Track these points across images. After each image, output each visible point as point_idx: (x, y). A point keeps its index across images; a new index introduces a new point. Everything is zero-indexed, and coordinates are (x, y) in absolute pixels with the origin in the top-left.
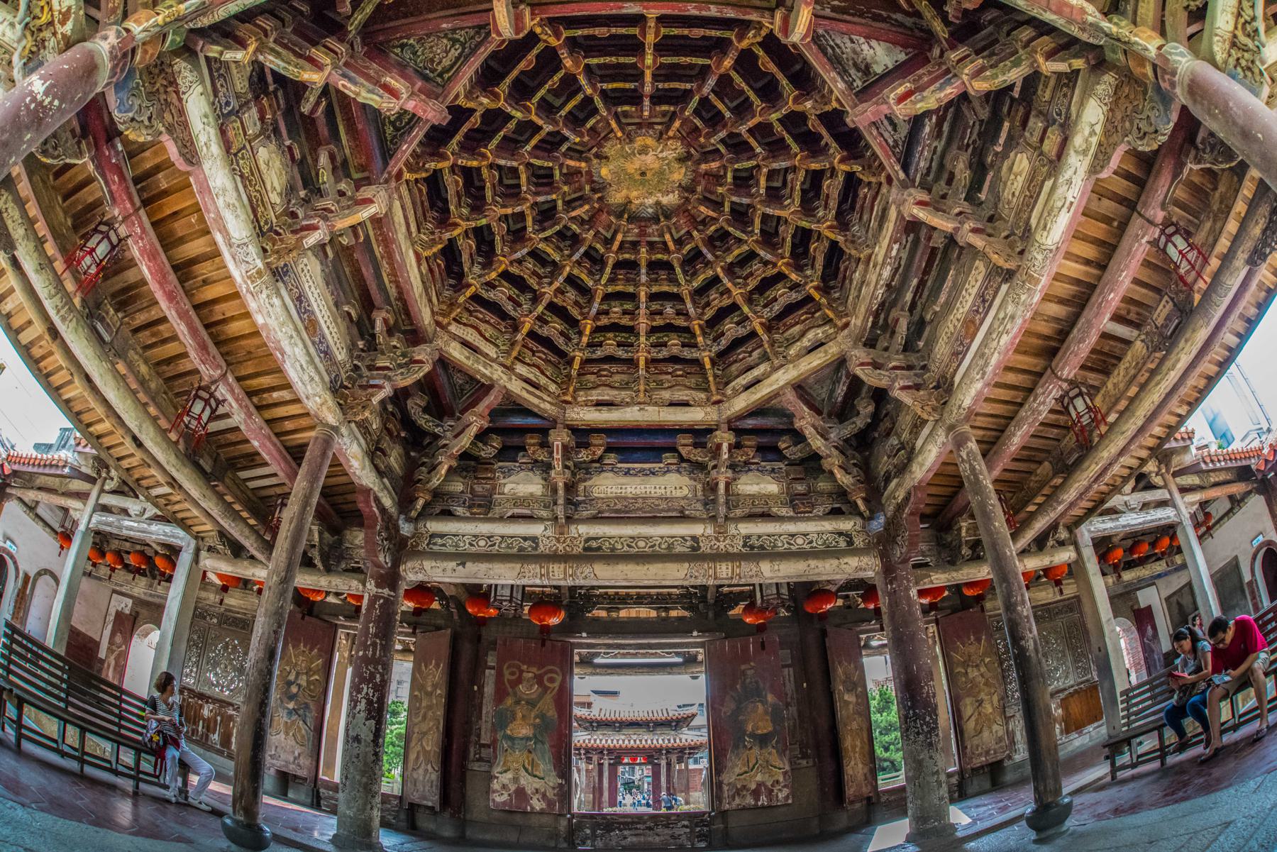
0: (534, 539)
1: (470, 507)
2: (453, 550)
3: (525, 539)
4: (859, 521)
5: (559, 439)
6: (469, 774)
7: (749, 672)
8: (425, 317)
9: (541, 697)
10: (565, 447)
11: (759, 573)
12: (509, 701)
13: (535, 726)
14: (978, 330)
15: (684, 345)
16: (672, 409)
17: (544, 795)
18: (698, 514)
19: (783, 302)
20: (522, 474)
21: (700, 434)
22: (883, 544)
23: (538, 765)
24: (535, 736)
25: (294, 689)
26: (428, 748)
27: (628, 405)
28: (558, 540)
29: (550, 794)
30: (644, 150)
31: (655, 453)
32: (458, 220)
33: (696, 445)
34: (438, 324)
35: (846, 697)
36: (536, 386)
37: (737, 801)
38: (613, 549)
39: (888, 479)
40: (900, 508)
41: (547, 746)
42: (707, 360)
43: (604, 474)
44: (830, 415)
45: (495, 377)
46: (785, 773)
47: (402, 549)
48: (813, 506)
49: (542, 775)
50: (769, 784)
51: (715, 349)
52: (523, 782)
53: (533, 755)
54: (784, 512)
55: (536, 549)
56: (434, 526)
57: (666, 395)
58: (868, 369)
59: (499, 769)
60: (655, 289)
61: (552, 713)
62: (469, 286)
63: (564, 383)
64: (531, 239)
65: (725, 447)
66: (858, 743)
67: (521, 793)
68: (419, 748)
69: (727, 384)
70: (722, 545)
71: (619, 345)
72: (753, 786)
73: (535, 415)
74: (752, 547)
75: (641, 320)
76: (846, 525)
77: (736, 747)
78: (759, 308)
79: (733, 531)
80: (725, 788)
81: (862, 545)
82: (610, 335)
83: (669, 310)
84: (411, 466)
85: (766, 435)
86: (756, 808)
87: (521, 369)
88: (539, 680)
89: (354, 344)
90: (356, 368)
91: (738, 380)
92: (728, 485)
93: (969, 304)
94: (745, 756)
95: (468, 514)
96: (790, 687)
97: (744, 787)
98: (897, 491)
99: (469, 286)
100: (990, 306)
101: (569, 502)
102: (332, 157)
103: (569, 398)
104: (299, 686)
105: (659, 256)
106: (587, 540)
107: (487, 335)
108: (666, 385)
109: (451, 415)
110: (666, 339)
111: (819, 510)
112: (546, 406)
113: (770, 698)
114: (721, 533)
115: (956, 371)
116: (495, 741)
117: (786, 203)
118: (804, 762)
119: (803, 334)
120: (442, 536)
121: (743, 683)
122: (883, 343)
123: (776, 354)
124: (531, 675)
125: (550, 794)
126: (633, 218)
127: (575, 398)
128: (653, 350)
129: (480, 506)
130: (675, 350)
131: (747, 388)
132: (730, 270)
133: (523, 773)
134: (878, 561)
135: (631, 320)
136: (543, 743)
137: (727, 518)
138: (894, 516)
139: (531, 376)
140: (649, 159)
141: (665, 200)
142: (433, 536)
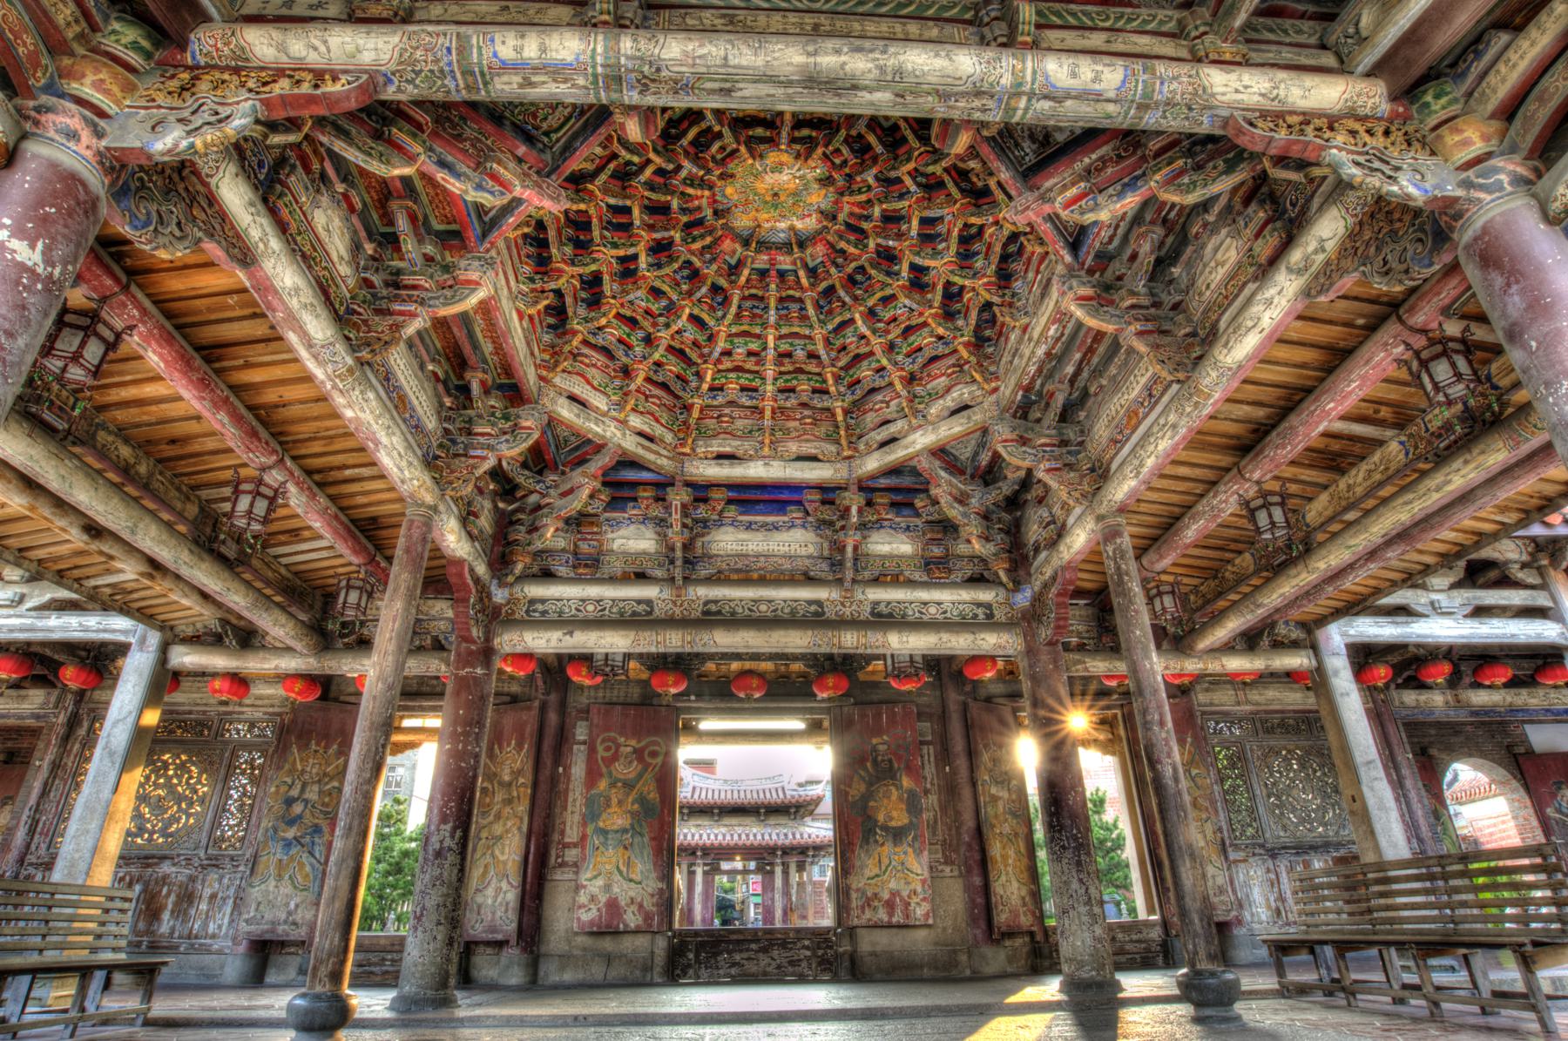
0: (649, 602)
1: (574, 567)
2: (555, 617)
3: (639, 602)
4: (1002, 593)
5: (678, 497)
8: (529, 376)
10: (684, 506)
12: (603, 784)
13: (633, 814)
14: (1140, 423)
15: (814, 391)
16: (799, 464)
17: (641, 906)
18: (823, 575)
19: (928, 353)
20: (632, 527)
21: (828, 493)
22: (1029, 619)
24: (632, 826)
25: (298, 808)
26: (502, 858)
27: (751, 459)
28: (674, 603)
29: (649, 904)
30: (778, 168)
31: (780, 506)
32: (562, 266)
33: (824, 502)
34: (541, 378)
35: (994, 791)
36: (650, 439)
37: (868, 914)
38: (733, 613)
39: (1037, 550)
40: (1046, 586)
41: (646, 839)
42: (839, 412)
43: (723, 529)
44: (973, 477)
45: (608, 434)
46: (923, 882)
47: (496, 618)
48: (950, 571)
49: (638, 878)
51: (849, 398)
54: (917, 576)
55: (650, 613)
56: (536, 590)
57: (794, 447)
58: (1012, 447)
59: (588, 875)
60: (784, 331)
61: (653, 796)
62: (575, 333)
63: (683, 430)
64: (644, 277)
65: (854, 510)
66: (1011, 853)
69: (860, 437)
70: (848, 611)
71: (743, 389)
72: (886, 896)
73: (649, 470)
74: (880, 615)
75: (768, 366)
76: (986, 595)
78: (900, 358)
79: (861, 597)
80: (854, 895)
81: (1003, 619)
82: (731, 375)
83: (800, 354)
84: (504, 523)
85: (900, 492)
87: (636, 421)
89: (441, 404)
90: (447, 431)
91: (872, 434)
92: (856, 548)
93: (1136, 392)
95: (572, 575)
98: (1047, 566)
99: (575, 333)
100: (1156, 403)
101: (686, 561)
102: (413, 218)
103: (687, 450)
104: (306, 801)
105: (791, 292)
106: (706, 603)
107: (595, 383)
108: (794, 434)
109: (554, 468)
110: (795, 382)
111: (957, 576)
112: (662, 461)
114: (847, 599)
115: (1112, 458)
116: (584, 837)
117: (940, 247)
118: (948, 869)
119: (948, 390)
120: (543, 601)
122: (1035, 414)
123: (916, 412)
126: (764, 245)
127: (693, 450)
128: (780, 396)
129: (586, 566)
130: (805, 398)
131: (883, 444)
132: (871, 314)
133: (617, 877)
134: (1021, 640)
135: (757, 364)
136: (642, 835)
137: (854, 581)
138: (1041, 593)
139: (646, 429)
140: (784, 177)
141: (799, 225)
142: (532, 602)
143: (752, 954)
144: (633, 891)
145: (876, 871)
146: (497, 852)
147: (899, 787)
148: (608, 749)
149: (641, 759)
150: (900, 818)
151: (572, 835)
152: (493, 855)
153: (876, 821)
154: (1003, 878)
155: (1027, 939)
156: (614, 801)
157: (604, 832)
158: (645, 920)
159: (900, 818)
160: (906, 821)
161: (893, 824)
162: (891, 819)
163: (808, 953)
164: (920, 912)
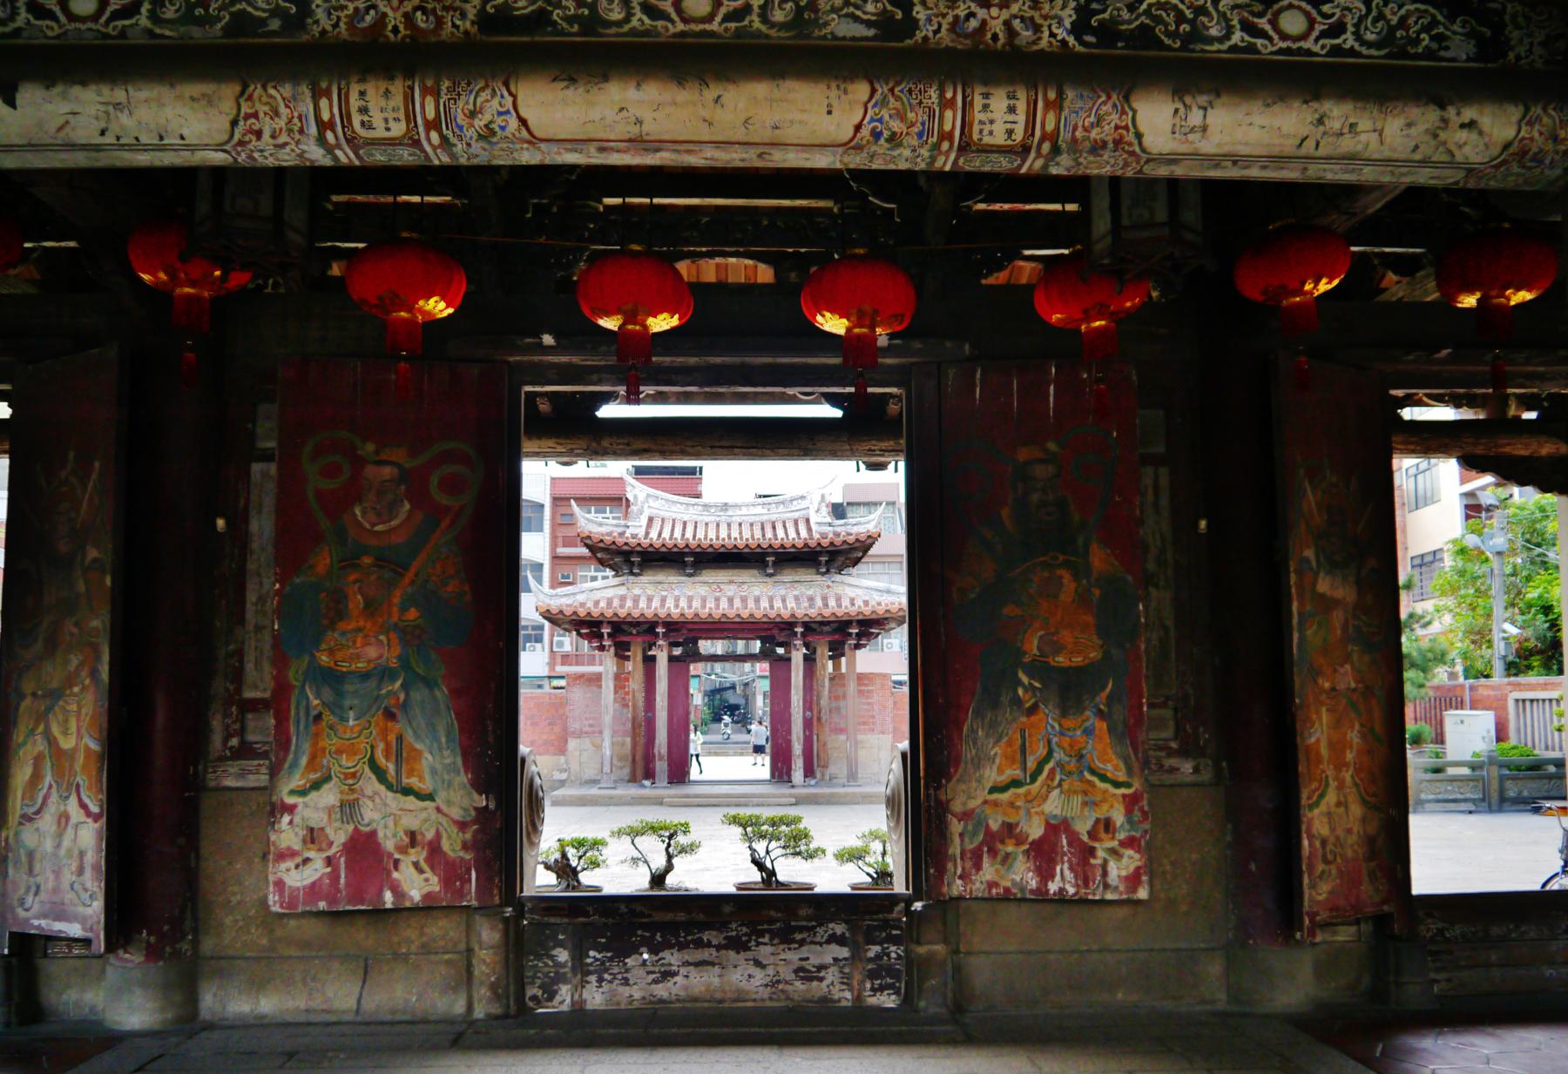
6: (208, 803)
7: (1041, 471)
11: (1127, 141)
12: (323, 560)
13: (408, 635)
17: (434, 849)
24: (405, 664)
26: (67, 744)
29: (452, 845)
35: (1323, 586)
37: (988, 871)
41: (442, 693)
46: (1131, 802)
49: (427, 785)
50: (1083, 827)
52: (370, 814)
53: (396, 727)
59: (297, 781)
66: (1354, 736)
67: (364, 852)
68: (40, 745)
72: (1036, 831)
74: (1108, 33)
80: (956, 827)
86: (1040, 897)
88: (414, 485)
96: (1155, 528)
97: (1009, 829)
113: (1099, 558)
116: (282, 690)
118: (1187, 767)
124: (387, 471)
125: (452, 845)
133: (370, 784)
136: (429, 684)
143: (705, 954)
144: (417, 816)
145: (1014, 772)
146: (55, 730)
149: (419, 497)
150: (1079, 649)
151: (258, 685)
152: (47, 734)
153: (1020, 653)
154: (1331, 797)
155: (1366, 928)
157: (332, 679)
158: (447, 882)
159: (1079, 649)
161: (1061, 660)
162: (1058, 649)
163: (844, 952)
164: (1116, 871)
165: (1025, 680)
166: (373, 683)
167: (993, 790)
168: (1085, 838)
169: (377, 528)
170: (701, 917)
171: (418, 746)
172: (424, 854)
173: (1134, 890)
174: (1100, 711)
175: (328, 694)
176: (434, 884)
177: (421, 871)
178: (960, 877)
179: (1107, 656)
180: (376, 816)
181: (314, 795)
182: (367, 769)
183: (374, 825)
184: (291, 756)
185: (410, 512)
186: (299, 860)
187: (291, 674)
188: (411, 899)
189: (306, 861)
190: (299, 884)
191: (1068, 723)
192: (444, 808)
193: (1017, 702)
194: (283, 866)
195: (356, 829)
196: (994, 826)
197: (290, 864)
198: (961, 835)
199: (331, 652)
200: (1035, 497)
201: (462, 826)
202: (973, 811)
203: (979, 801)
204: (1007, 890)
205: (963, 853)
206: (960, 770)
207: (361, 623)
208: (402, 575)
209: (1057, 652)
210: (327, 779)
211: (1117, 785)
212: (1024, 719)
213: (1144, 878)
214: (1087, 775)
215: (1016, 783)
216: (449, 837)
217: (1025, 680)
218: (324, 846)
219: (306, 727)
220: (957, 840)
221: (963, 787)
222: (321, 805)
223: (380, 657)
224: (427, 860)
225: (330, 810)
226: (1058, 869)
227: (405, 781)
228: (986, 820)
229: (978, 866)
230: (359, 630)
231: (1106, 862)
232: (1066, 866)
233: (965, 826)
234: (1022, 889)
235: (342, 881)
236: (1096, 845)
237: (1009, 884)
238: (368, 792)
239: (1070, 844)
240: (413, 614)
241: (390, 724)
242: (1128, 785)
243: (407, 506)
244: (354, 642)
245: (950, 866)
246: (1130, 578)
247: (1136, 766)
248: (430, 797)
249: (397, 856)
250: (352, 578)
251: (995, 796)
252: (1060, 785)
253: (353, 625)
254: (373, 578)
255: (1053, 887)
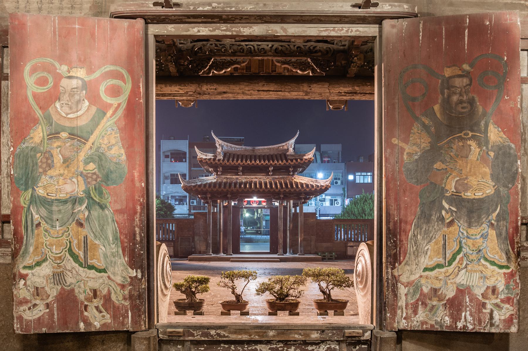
9: (95, 122)
17: (107, 299)
23: (95, 247)
29: (118, 298)
49: (101, 265)
67: (68, 301)
72: (450, 293)
77: (425, 217)
94: (439, 236)
121: (447, 102)
124: (74, 83)
133: (70, 263)
136: (102, 207)
145: (441, 260)
147: (483, 142)
148: (42, 82)
149: (94, 99)
156: (58, 159)
158: (114, 317)
160: (490, 191)
161: (469, 195)
162: (467, 188)
165: (447, 206)
166: (69, 206)
167: (426, 269)
168: (480, 298)
169: (69, 116)
170: (257, 338)
171: (97, 242)
172: (102, 302)
173: (509, 327)
174: (492, 224)
175: (44, 212)
176: (108, 319)
177: (101, 312)
178: (405, 318)
179: (497, 191)
180: (73, 281)
181: (38, 268)
182: (68, 255)
183: (73, 286)
184: (23, 247)
185: (89, 106)
186: (29, 305)
187: (22, 200)
188: (95, 326)
189: (35, 305)
190: (30, 318)
191: (472, 231)
192: (112, 277)
193: (442, 219)
194: (22, 308)
195: (62, 288)
196: (426, 290)
197: (25, 307)
198: (406, 295)
199: (45, 188)
200: (455, 98)
201: (123, 287)
202: (413, 281)
203: (417, 276)
204: (432, 326)
205: (407, 305)
206: (407, 259)
207: (62, 172)
208: (85, 144)
209: (466, 190)
210: (45, 260)
211: (501, 267)
212: (445, 229)
213: (515, 321)
214: (482, 261)
215: (439, 266)
216: (116, 293)
217: (447, 206)
218: (44, 297)
219: (32, 230)
220: (404, 298)
221: (408, 268)
222: (42, 275)
223: (72, 192)
224: (103, 305)
225: (47, 277)
226: (463, 314)
227: (90, 262)
228: (421, 286)
229: (415, 312)
230: (61, 175)
231: (492, 311)
232: (468, 313)
233: (409, 291)
234: (441, 326)
235: (56, 317)
236: (487, 301)
237: (433, 323)
238: (69, 267)
239: (471, 301)
240: (92, 166)
241: (80, 229)
242: (507, 267)
243: (87, 103)
244: (58, 182)
245: (399, 312)
246: (513, 146)
247: (513, 256)
248: (104, 271)
249: (86, 303)
250: (55, 145)
251: (427, 273)
252: (466, 267)
253: (57, 172)
254: (68, 144)
255: (460, 325)
